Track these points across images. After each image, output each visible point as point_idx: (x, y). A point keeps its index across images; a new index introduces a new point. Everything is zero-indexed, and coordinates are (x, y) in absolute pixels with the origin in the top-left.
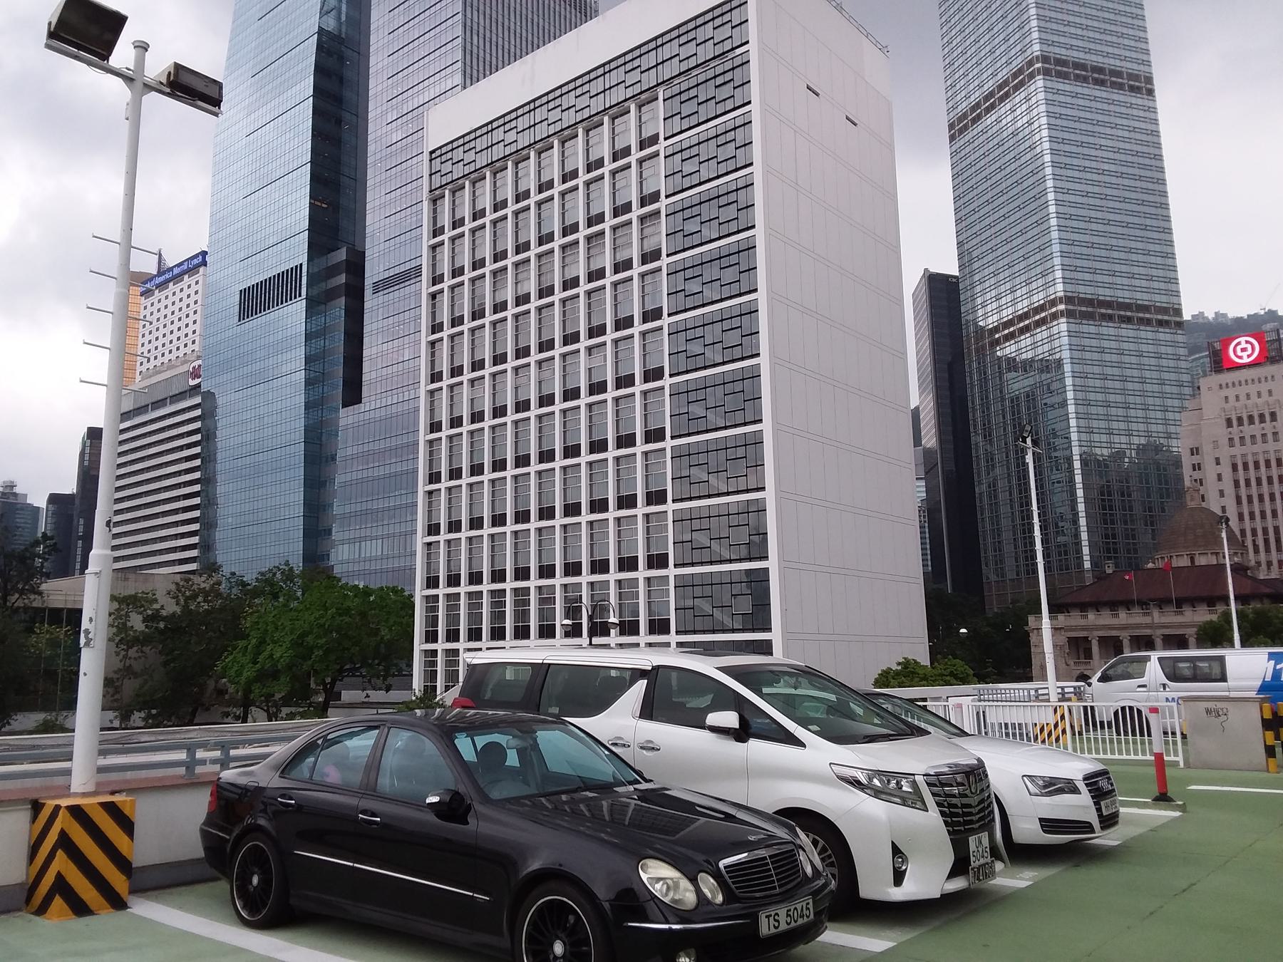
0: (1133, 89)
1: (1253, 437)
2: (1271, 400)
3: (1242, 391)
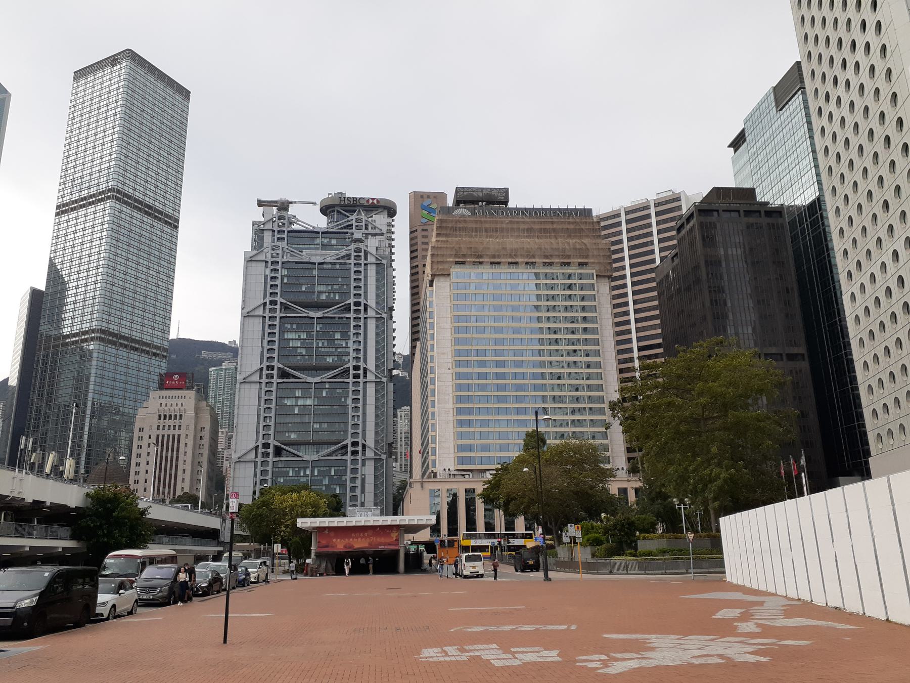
0: (166, 222)
1: (169, 426)
2: (182, 408)
3: (169, 401)
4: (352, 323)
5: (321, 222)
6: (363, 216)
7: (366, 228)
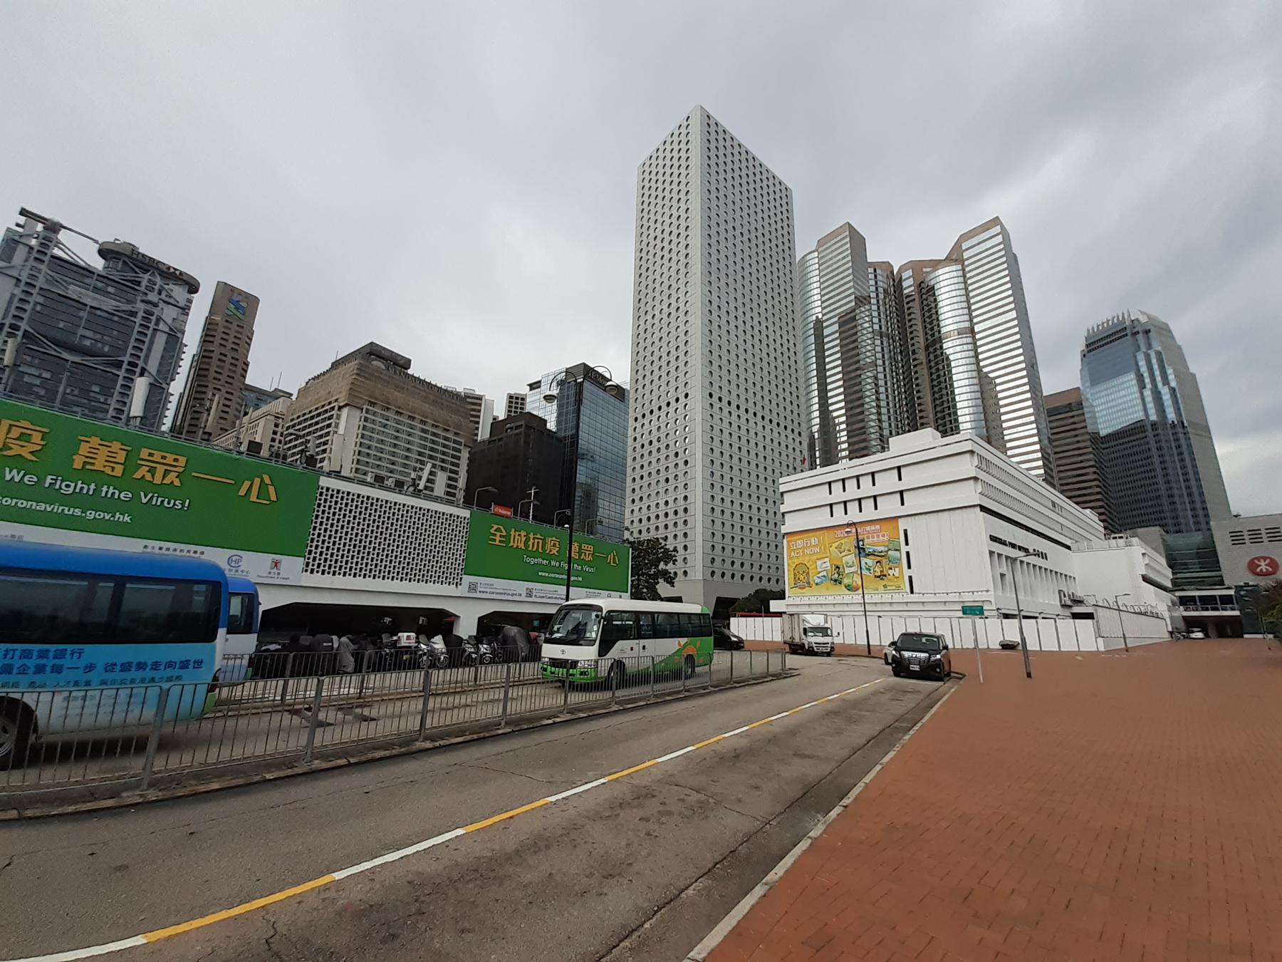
4: (120, 382)
5: (98, 264)
6: (158, 280)
7: (160, 293)
